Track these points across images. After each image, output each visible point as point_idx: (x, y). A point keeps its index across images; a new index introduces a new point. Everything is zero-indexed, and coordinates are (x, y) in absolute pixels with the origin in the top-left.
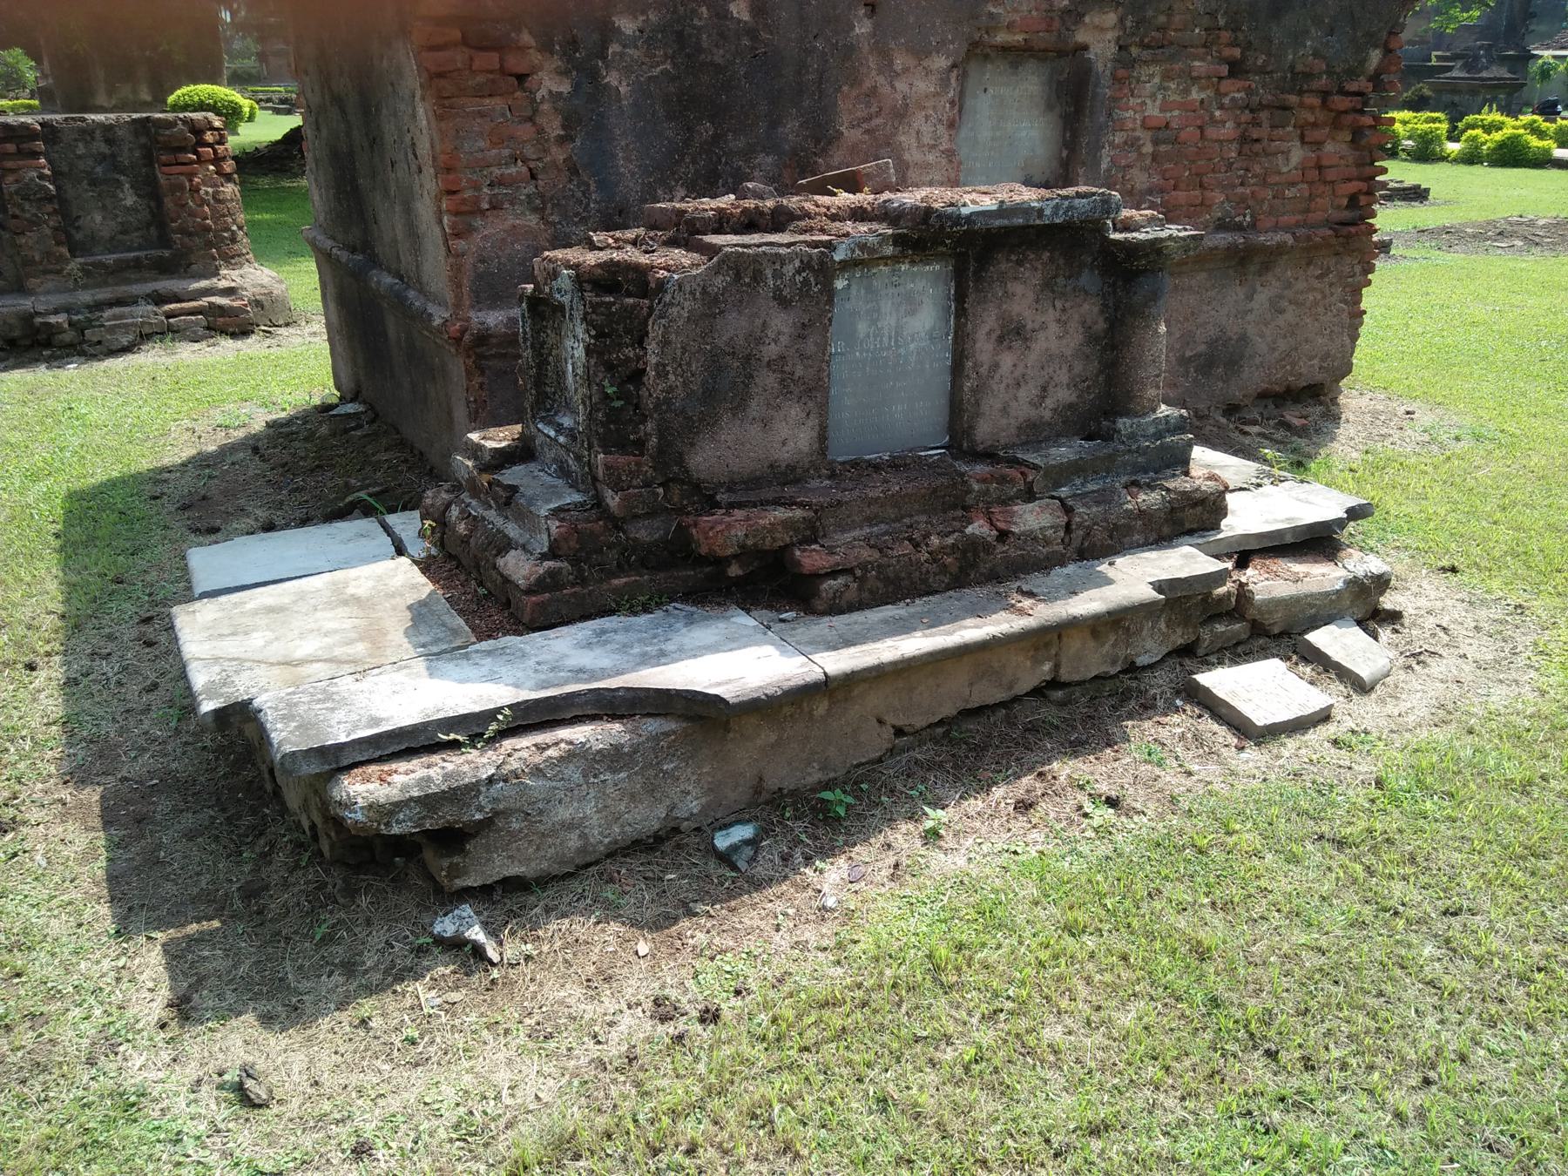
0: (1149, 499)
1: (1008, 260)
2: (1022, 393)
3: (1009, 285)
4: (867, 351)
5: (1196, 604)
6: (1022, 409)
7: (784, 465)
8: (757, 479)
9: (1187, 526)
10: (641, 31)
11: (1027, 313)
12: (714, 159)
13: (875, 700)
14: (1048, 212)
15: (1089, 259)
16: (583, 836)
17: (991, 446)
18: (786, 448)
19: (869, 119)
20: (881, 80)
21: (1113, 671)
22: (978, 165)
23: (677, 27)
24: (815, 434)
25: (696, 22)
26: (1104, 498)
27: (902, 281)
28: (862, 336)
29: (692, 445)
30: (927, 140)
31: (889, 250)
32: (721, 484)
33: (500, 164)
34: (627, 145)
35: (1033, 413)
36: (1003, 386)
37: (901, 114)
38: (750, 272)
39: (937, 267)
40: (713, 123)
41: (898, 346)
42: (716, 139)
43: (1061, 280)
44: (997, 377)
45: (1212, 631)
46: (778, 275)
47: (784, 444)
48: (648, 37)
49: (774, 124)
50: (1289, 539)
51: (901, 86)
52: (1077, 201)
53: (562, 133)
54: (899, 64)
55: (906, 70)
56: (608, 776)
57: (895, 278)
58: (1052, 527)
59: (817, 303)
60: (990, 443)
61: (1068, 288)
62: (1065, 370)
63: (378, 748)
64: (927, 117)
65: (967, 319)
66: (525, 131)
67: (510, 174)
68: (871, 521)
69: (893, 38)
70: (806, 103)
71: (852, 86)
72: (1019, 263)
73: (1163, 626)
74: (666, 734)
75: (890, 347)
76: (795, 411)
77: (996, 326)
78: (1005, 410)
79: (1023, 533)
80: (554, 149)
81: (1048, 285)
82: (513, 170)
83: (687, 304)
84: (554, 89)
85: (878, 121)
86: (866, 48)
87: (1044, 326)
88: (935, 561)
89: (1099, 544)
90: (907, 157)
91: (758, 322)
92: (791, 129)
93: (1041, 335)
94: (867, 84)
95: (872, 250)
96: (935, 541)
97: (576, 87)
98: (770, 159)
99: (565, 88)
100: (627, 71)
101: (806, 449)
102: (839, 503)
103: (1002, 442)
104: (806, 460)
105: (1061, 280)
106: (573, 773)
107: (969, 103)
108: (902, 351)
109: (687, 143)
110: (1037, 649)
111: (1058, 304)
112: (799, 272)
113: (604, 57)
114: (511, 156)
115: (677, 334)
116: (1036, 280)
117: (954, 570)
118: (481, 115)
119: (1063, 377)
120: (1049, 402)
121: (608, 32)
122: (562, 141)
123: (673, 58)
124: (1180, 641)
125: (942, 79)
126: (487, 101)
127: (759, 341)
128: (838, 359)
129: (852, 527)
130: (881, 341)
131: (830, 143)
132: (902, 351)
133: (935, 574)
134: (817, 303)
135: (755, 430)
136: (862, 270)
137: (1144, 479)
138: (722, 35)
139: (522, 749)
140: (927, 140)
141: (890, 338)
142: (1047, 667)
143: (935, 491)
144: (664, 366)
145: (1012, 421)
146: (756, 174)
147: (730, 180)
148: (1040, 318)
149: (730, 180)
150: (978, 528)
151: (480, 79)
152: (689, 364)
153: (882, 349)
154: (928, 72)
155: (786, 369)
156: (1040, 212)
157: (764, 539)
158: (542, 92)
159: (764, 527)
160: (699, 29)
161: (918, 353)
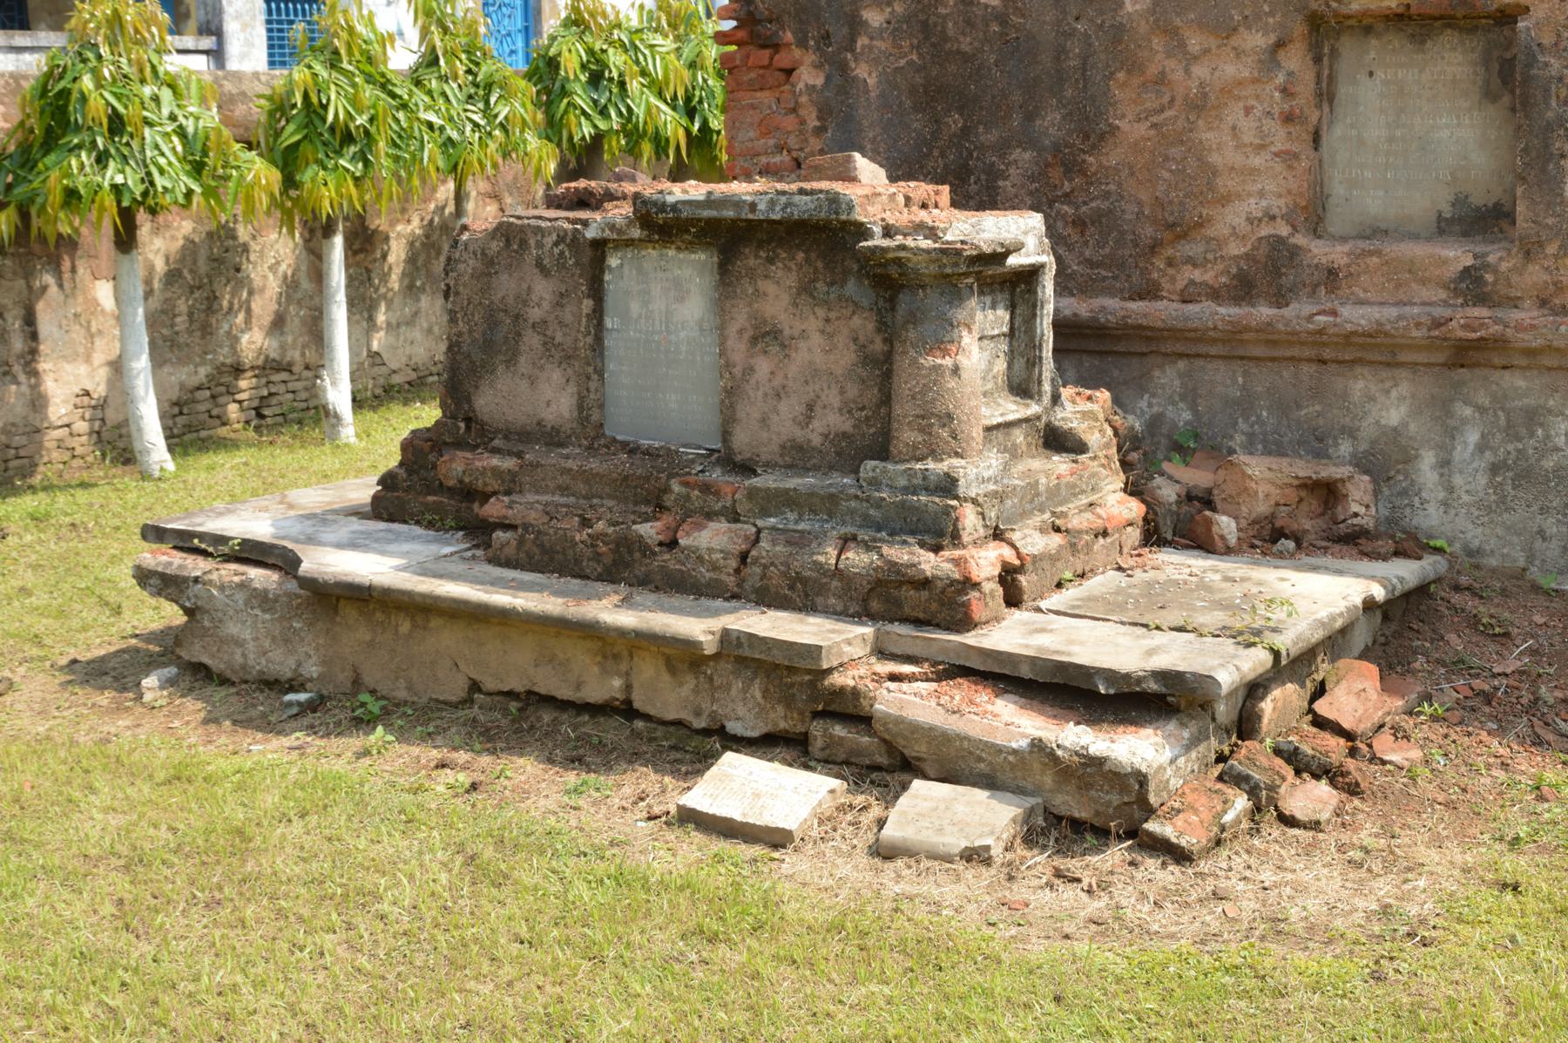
0: (857, 559)
1: (757, 257)
2: (783, 407)
3: (759, 283)
4: (640, 332)
5: (801, 684)
6: (785, 423)
7: (549, 426)
8: (529, 433)
9: (907, 610)
10: (889, 23)
11: (782, 317)
12: (965, 154)
13: (446, 639)
14: (762, 207)
15: (855, 267)
16: (244, 655)
17: (751, 459)
18: (550, 410)
19: (1162, 110)
20: (1171, 64)
21: (700, 723)
22: (1367, 174)
23: (922, 17)
24: (574, 401)
25: (942, 10)
26: (799, 541)
28: (635, 315)
29: (477, 387)
30: (1249, 137)
31: (636, 233)
32: (498, 431)
33: (766, 153)
34: (875, 138)
35: (799, 434)
36: (760, 393)
37: (1199, 105)
38: (517, 240)
39: (703, 257)
40: (961, 115)
41: (669, 332)
42: (966, 131)
43: (821, 286)
44: (753, 381)
45: (826, 730)
46: (539, 245)
47: (548, 403)
48: (894, 29)
49: (1030, 117)
50: (1025, 672)
51: (1200, 71)
52: (797, 198)
53: (818, 124)
54: (1195, 43)
55: (1207, 51)
56: (257, 612)
57: (663, 263)
58: (722, 551)
59: (573, 276)
60: (749, 455)
61: (832, 296)
62: (835, 391)
63: (182, 540)
64: (1248, 111)
66: (789, 122)
67: (775, 164)
68: (564, 490)
69: (1178, 14)
70: (1069, 93)
71: (1129, 72)
72: (771, 261)
73: (758, 695)
74: (298, 596)
75: (661, 332)
76: (556, 375)
77: (747, 325)
78: (764, 421)
79: (687, 548)
80: (812, 140)
81: (806, 289)
82: (777, 159)
83: (471, 262)
84: (811, 82)
85: (1169, 113)
86: (1143, 28)
87: (804, 334)
88: (593, 546)
89: (773, 590)
90: (1215, 158)
91: (525, 286)
92: (1052, 123)
93: (802, 345)
94: (1152, 70)
95: (620, 232)
96: (600, 526)
97: (828, 78)
98: (1027, 155)
99: (819, 81)
100: (876, 61)
101: (567, 415)
102: (538, 465)
103: (764, 458)
104: (569, 426)
105: (821, 286)
106: (240, 597)
107: (1343, 90)
108: (673, 337)
109: (935, 135)
110: (605, 657)
111: (821, 312)
112: (556, 244)
113: (853, 50)
114: (776, 146)
115: (465, 286)
116: (791, 280)
117: (608, 560)
118: (753, 107)
119: (834, 399)
120: (818, 425)
121: (855, 25)
122: (819, 131)
123: (918, 47)
124: (783, 725)
125: (1260, 61)
126: (759, 94)
127: (525, 303)
128: (615, 335)
129: (546, 490)
130: (653, 325)
131: (1102, 137)
132: (673, 337)
133: (589, 560)
134: (573, 276)
135: (524, 385)
137: (863, 535)
138: (969, 23)
139: (230, 572)
140: (1249, 137)
142: (617, 683)
143: (626, 478)
144: (456, 312)
145: (774, 437)
146: (1011, 171)
147: (983, 177)
148: (799, 326)
149: (983, 177)
150: (649, 531)
151: (753, 75)
152: (473, 315)
154: (1238, 53)
155: (548, 333)
156: (753, 206)
157: (477, 479)
158: (801, 86)
159: (477, 469)
160: (945, 17)
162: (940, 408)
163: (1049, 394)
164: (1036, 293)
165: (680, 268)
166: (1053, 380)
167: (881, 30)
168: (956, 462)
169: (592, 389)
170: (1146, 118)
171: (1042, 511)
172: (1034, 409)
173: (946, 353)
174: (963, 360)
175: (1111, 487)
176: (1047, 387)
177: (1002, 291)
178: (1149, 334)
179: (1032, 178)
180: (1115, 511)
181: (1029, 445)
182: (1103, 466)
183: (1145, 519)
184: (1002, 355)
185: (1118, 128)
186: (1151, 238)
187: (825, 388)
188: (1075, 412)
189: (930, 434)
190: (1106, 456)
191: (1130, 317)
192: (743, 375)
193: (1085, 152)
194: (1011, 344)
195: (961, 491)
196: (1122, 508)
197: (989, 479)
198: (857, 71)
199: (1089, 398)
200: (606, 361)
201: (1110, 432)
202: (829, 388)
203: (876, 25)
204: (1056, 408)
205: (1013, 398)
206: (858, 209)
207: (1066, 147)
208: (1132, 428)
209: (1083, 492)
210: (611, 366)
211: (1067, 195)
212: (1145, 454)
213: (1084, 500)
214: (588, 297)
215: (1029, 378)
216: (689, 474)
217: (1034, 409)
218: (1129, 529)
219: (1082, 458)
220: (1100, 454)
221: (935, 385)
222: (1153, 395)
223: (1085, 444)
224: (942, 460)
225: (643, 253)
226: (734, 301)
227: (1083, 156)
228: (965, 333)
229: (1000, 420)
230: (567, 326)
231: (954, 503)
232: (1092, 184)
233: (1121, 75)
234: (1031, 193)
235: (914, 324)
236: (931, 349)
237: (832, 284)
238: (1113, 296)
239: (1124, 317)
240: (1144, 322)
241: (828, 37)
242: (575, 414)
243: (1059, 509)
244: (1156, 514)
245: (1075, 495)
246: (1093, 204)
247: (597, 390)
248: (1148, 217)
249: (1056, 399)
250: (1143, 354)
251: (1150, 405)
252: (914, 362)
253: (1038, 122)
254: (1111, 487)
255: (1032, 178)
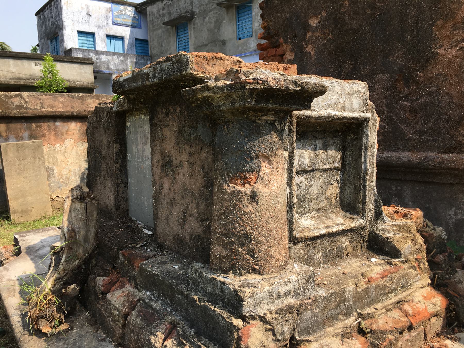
10: (320, 23)
23: (334, 16)
36: (166, 202)
40: (352, 61)
48: (322, 26)
61: (192, 136)
71: (445, 19)
98: (384, 77)
113: (305, 40)
121: (306, 27)
131: (427, 60)
146: (376, 86)
160: (344, 13)
162: (239, 229)
163: (373, 212)
164: (361, 140)
166: (376, 202)
167: (317, 27)
168: (251, 278)
169: (121, 192)
170: (456, 46)
171: (348, 314)
172: (359, 222)
173: (245, 181)
174: (261, 188)
175: (419, 284)
176: (371, 206)
177: (334, 137)
178: (455, 172)
179: (387, 89)
180: (421, 306)
181: (354, 248)
182: (414, 267)
183: (448, 309)
184: (335, 183)
185: (438, 53)
186: (458, 116)
187: (190, 202)
188: (393, 225)
189: (231, 250)
190: (416, 259)
191: (443, 162)
193: (416, 70)
194: (343, 176)
195: (246, 311)
196: (428, 303)
197: (287, 294)
198: (307, 49)
199: (405, 216)
201: (420, 240)
202: (192, 202)
203: (315, 25)
204: (378, 221)
205: (344, 213)
206: (191, 65)
207: (406, 69)
208: (440, 237)
209: (393, 290)
210: (130, 180)
211: (406, 96)
212: (450, 256)
213: (393, 299)
214: (116, 143)
215: (356, 200)
216: (134, 247)
217: (359, 222)
218: (433, 320)
219: (395, 261)
220: (411, 258)
221: (234, 208)
222: (458, 208)
223: (398, 251)
224: (241, 275)
227: (416, 73)
228: (264, 164)
229: (323, 232)
231: (237, 322)
232: (421, 88)
233: (440, 23)
234: (386, 97)
235: (222, 155)
236: (234, 177)
237: (191, 128)
238: (433, 151)
239: (439, 162)
240: (453, 166)
241: (296, 36)
243: (365, 312)
244: (457, 305)
245: (385, 294)
246: (422, 100)
247: (123, 193)
248: (456, 104)
249: (378, 215)
250: (452, 184)
251: (456, 214)
252: (221, 187)
253: (390, 58)
254: (419, 284)
255: (387, 89)
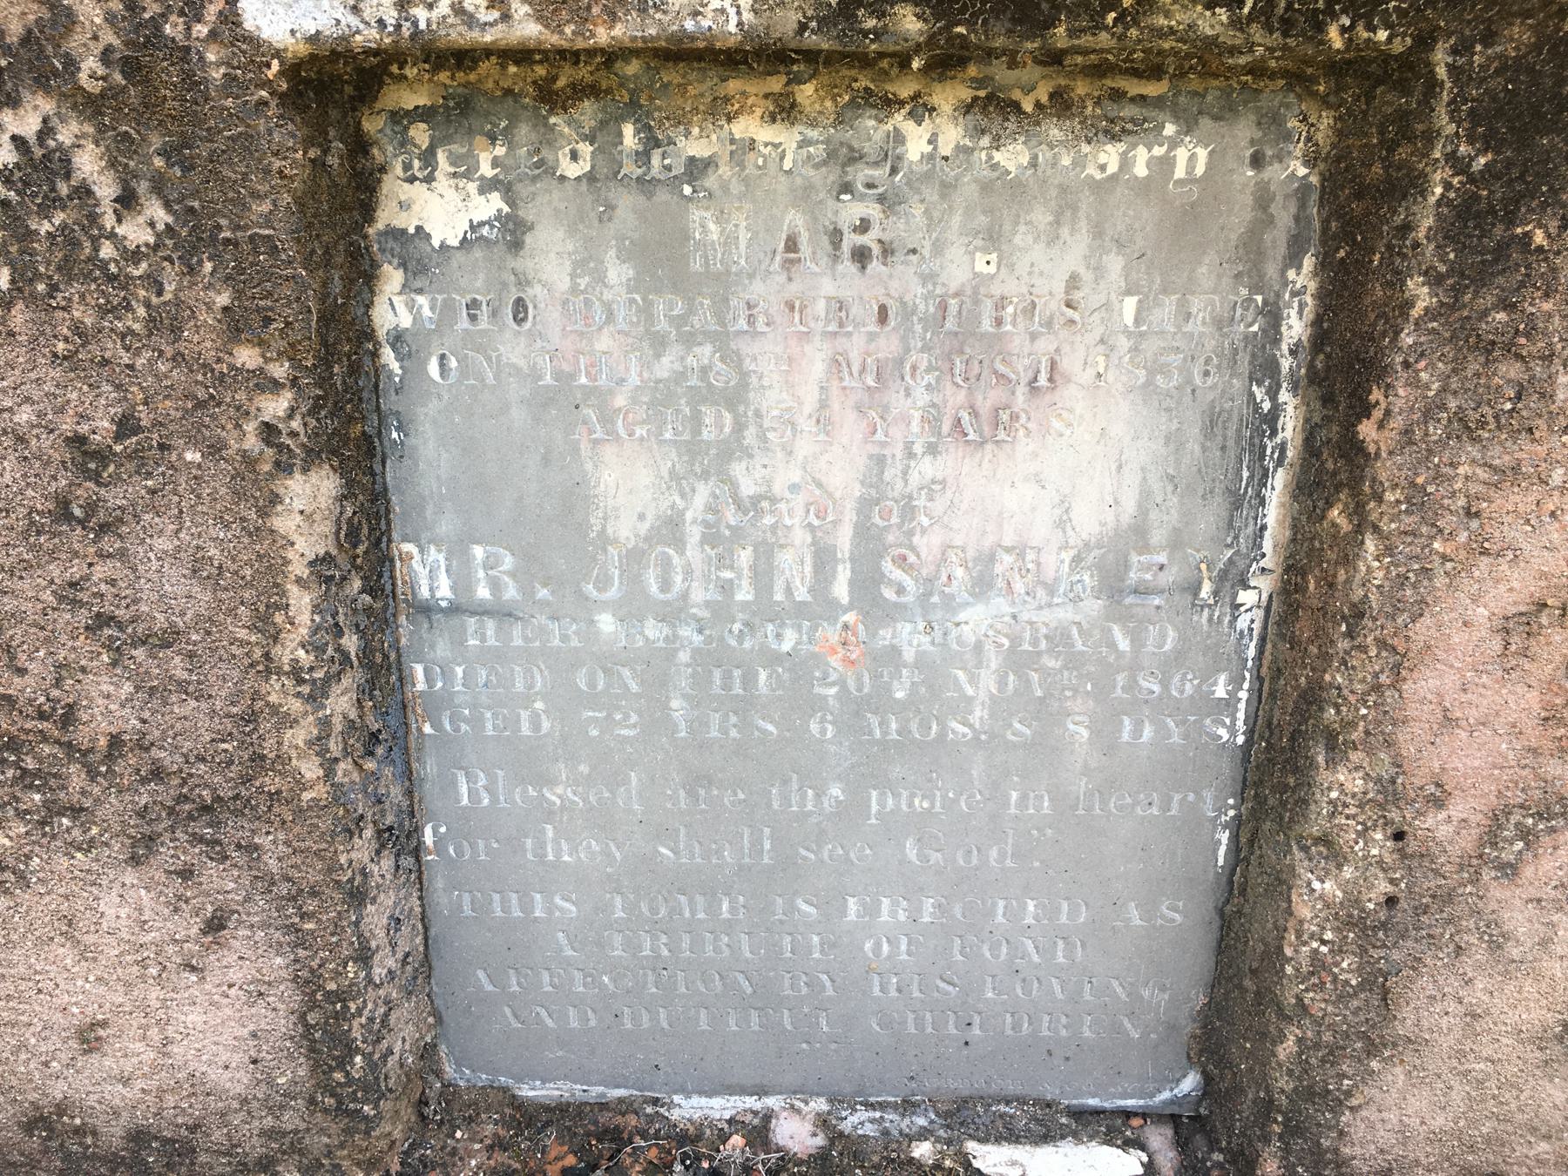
4: (672, 613)
27: (911, 224)
28: (625, 529)
47: (90, 1037)
57: (852, 211)
59: (166, 322)
65: (1362, 523)
75: (821, 607)
108: (909, 637)
130: (763, 575)
132: (909, 637)
136: (603, 135)
141: (823, 560)
153: (765, 611)
161: (1018, 661)
165: (993, 239)
192: (1492, 836)
200: (429, 768)
225: (695, 146)
226: (1526, 451)
230: (168, 639)
242: (292, 1072)
